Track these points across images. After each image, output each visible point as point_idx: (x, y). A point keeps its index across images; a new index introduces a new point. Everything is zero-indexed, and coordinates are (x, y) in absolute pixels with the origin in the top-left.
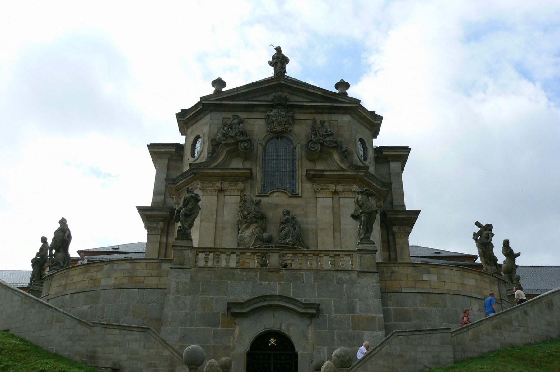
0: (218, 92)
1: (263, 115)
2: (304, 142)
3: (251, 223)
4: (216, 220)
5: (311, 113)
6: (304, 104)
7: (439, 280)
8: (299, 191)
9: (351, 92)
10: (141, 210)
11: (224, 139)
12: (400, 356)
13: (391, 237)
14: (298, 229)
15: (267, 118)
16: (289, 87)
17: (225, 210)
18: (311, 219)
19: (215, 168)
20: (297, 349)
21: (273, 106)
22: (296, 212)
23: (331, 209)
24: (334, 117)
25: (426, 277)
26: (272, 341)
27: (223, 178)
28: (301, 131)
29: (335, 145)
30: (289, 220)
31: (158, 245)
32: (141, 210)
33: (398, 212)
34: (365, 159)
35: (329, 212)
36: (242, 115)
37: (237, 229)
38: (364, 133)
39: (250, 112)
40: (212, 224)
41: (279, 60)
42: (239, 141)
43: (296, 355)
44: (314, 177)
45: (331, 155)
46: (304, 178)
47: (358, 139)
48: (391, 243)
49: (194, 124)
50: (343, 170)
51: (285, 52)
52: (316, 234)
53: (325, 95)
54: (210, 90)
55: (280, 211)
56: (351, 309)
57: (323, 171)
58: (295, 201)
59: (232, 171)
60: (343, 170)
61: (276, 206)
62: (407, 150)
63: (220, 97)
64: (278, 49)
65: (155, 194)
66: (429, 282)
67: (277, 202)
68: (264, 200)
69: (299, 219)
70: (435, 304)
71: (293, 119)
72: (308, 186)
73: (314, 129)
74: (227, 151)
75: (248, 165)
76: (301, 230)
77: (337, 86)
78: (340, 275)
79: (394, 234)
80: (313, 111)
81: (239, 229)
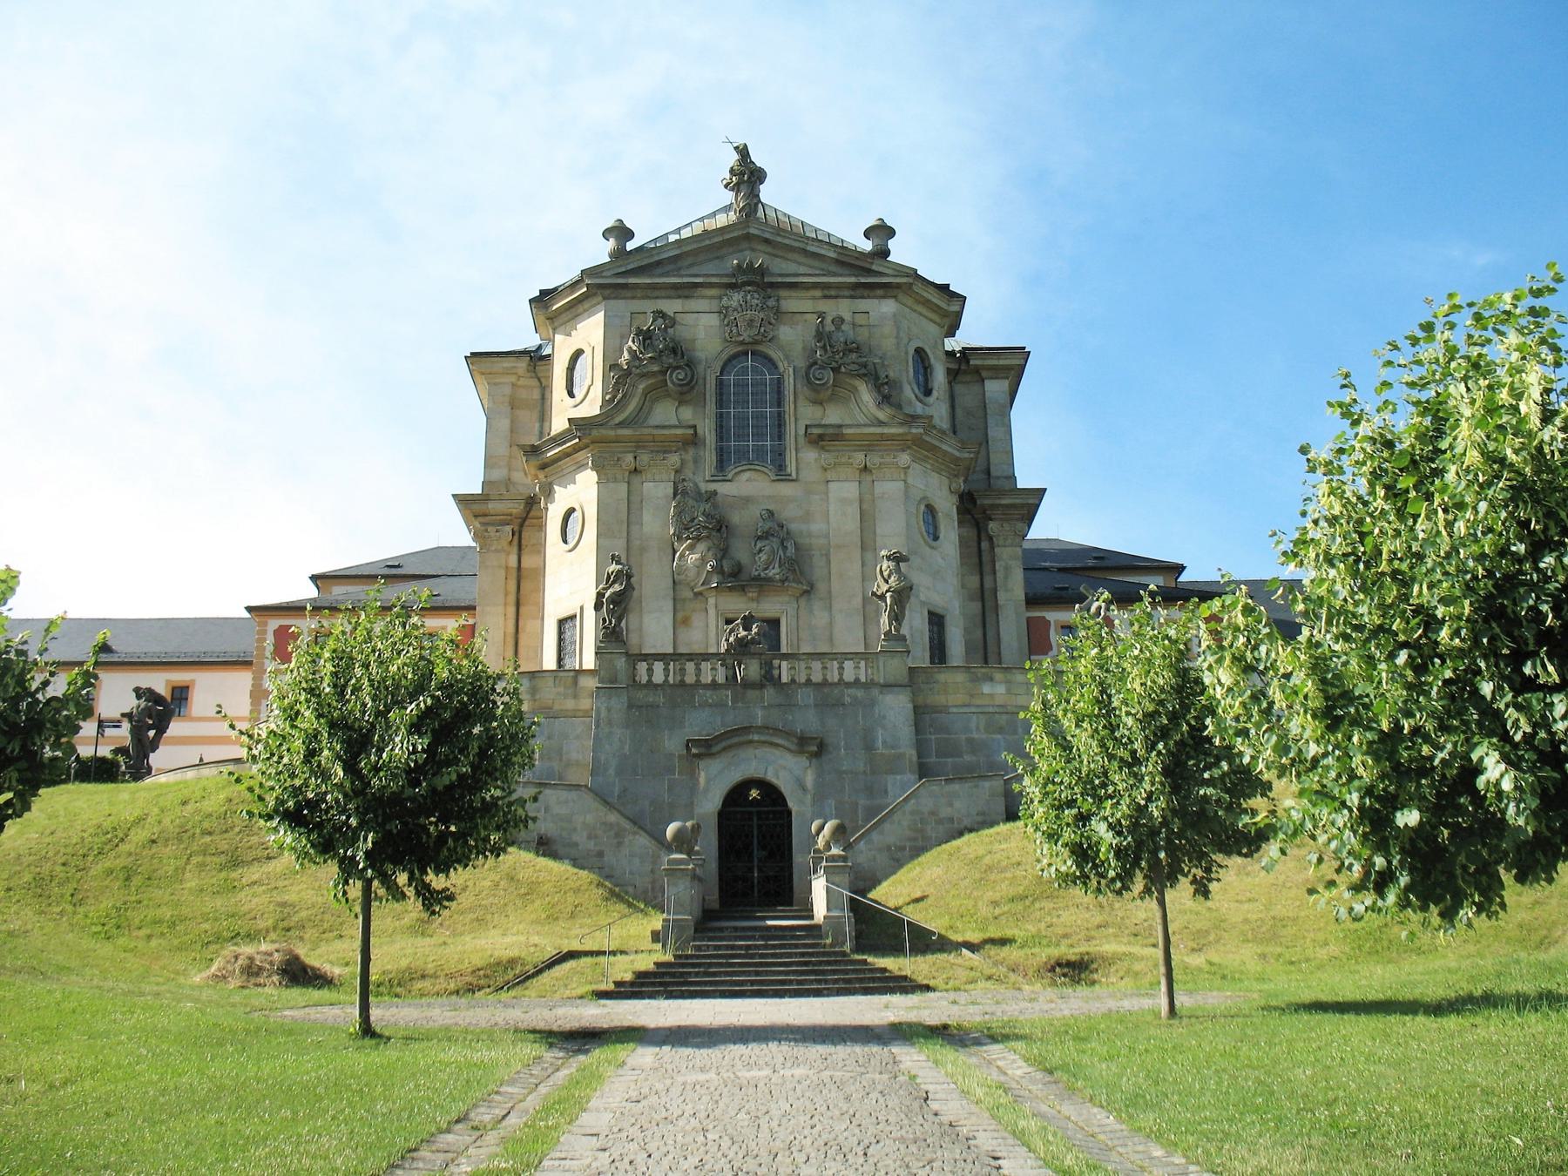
0: (619, 254)
1: (715, 305)
2: (801, 363)
3: (698, 539)
5: (814, 298)
7: (1009, 692)
8: (791, 468)
9: (900, 252)
10: (463, 501)
12: (933, 813)
13: (985, 545)
14: (791, 550)
15: (723, 312)
16: (767, 241)
18: (816, 527)
19: (621, 425)
20: (790, 804)
21: (733, 286)
22: (788, 513)
23: (857, 505)
24: (863, 305)
25: (986, 689)
26: (754, 793)
27: (639, 444)
28: (793, 339)
29: (863, 371)
30: (774, 530)
31: (503, 572)
32: (463, 501)
33: (1003, 493)
34: (928, 392)
35: (853, 511)
36: (670, 306)
38: (924, 330)
39: (687, 297)
41: (747, 176)
43: (789, 813)
44: (822, 438)
45: (854, 391)
46: (801, 440)
47: (911, 351)
48: (986, 558)
50: (881, 423)
51: (758, 158)
52: (827, 555)
53: (846, 258)
54: (600, 252)
55: (755, 511)
56: (869, 747)
57: (840, 426)
58: (785, 489)
59: (655, 432)
60: (881, 423)
61: (747, 500)
62: (1022, 354)
64: (743, 152)
65: (489, 463)
66: (991, 696)
67: (748, 489)
68: (723, 488)
69: (793, 527)
70: (1001, 730)
71: (778, 312)
72: (810, 455)
73: (820, 335)
75: (687, 414)
76: (797, 549)
77: (868, 234)
78: (851, 691)
79: (991, 539)
80: (818, 293)
81: (675, 552)
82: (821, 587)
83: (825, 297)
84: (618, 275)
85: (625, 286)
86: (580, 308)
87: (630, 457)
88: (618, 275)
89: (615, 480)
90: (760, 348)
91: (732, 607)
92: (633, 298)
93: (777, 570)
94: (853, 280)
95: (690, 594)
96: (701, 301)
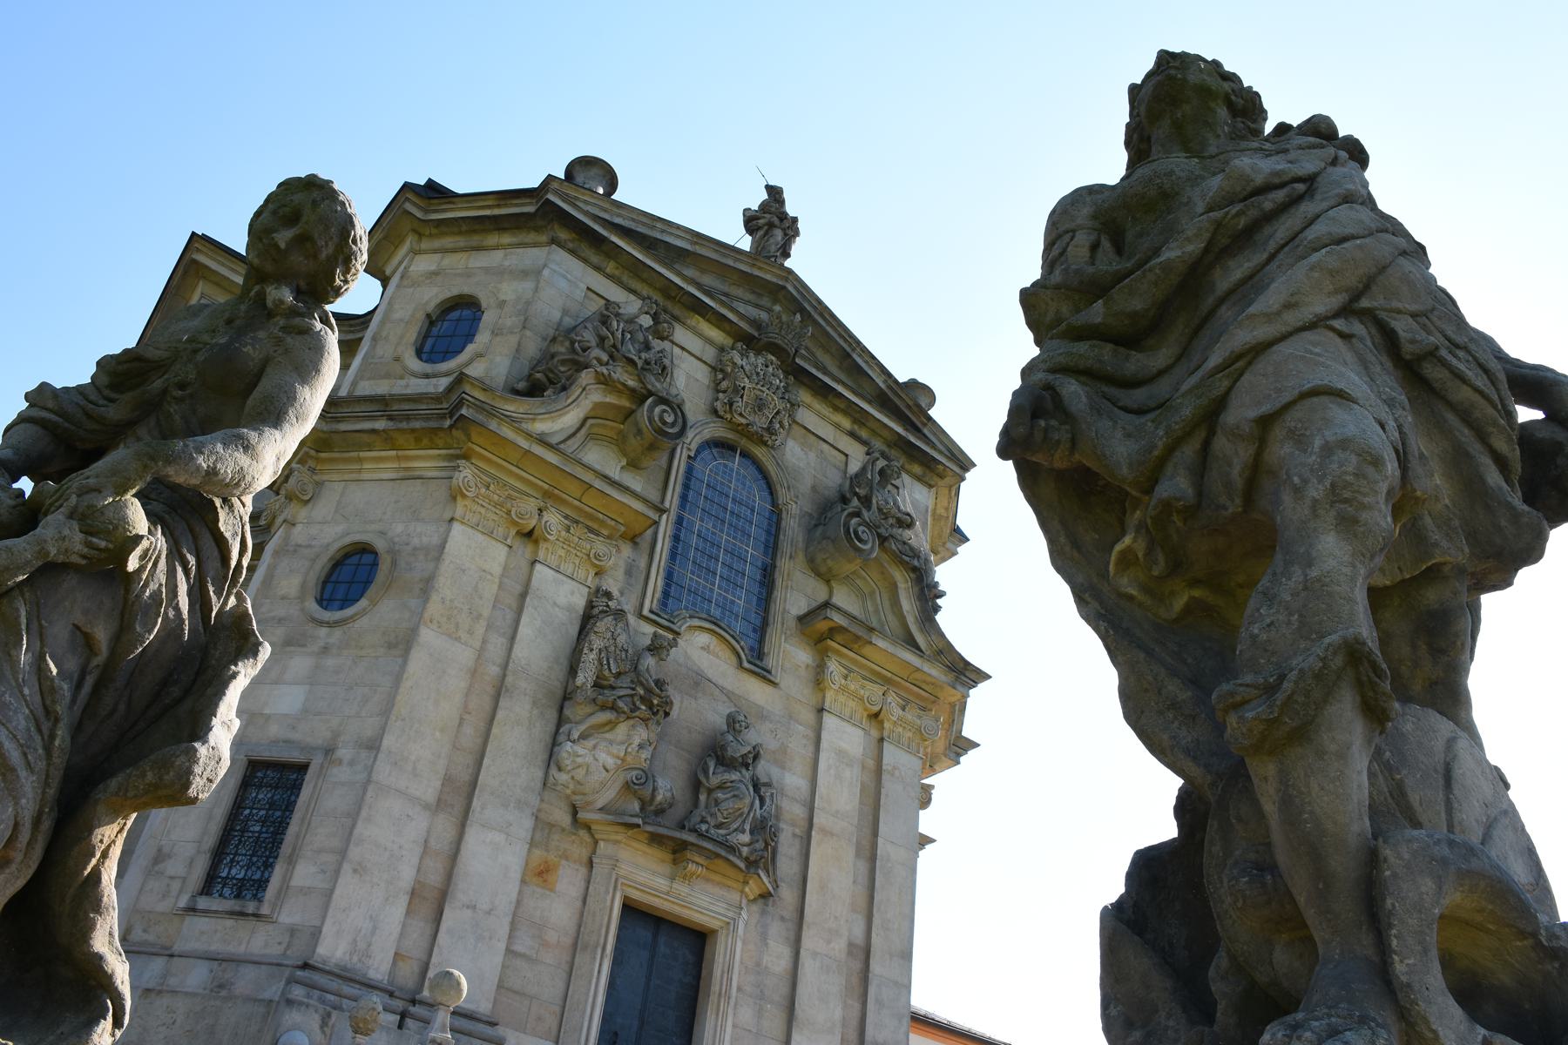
4: (484, 642)
5: (837, 426)
6: (840, 388)
8: (770, 662)
11: (605, 357)
17: (525, 619)
19: (542, 440)
30: (724, 755)
37: (552, 715)
40: (464, 655)
42: (651, 394)
49: (454, 251)
58: (754, 691)
63: (606, 216)
64: (775, 193)
74: (597, 406)
80: (846, 423)
82: (787, 894)
83: (852, 434)
84: (596, 218)
85: (597, 241)
86: (492, 239)
87: (531, 505)
88: (596, 218)
89: (490, 534)
90: (759, 452)
91: (643, 877)
92: (597, 268)
93: (746, 838)
94: (899, 430)
95: (564, 819)
96: (690, 334)
